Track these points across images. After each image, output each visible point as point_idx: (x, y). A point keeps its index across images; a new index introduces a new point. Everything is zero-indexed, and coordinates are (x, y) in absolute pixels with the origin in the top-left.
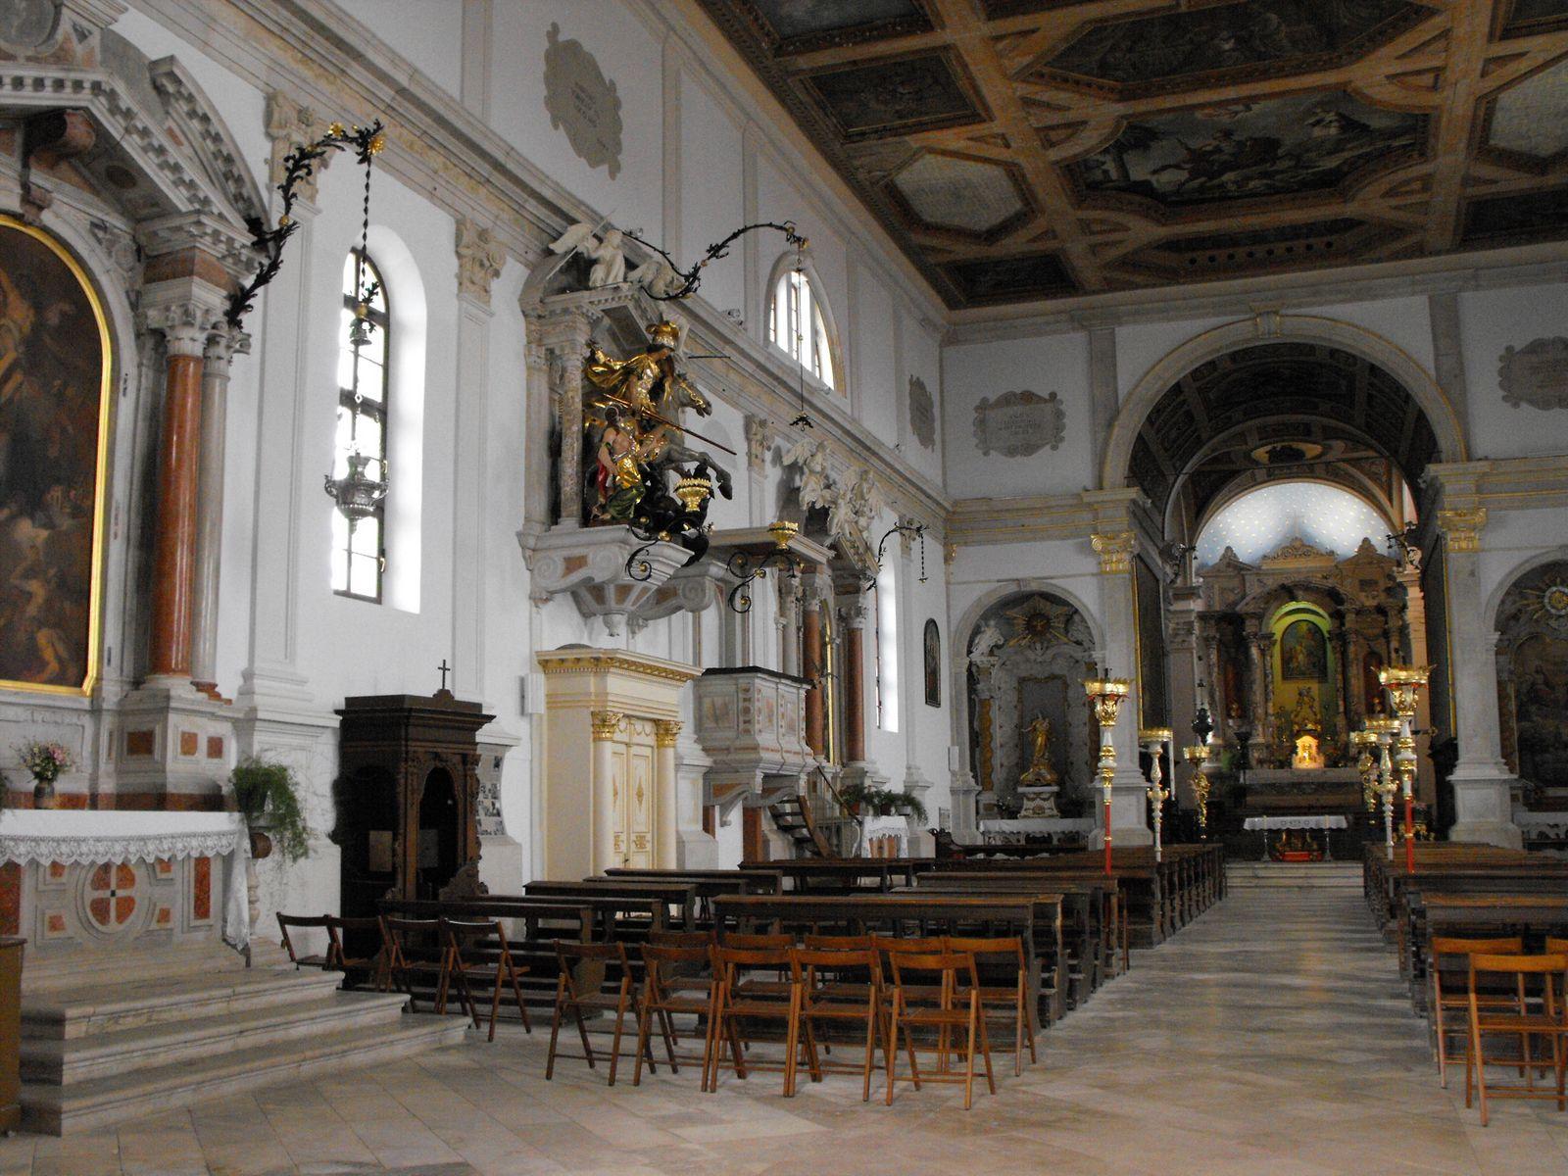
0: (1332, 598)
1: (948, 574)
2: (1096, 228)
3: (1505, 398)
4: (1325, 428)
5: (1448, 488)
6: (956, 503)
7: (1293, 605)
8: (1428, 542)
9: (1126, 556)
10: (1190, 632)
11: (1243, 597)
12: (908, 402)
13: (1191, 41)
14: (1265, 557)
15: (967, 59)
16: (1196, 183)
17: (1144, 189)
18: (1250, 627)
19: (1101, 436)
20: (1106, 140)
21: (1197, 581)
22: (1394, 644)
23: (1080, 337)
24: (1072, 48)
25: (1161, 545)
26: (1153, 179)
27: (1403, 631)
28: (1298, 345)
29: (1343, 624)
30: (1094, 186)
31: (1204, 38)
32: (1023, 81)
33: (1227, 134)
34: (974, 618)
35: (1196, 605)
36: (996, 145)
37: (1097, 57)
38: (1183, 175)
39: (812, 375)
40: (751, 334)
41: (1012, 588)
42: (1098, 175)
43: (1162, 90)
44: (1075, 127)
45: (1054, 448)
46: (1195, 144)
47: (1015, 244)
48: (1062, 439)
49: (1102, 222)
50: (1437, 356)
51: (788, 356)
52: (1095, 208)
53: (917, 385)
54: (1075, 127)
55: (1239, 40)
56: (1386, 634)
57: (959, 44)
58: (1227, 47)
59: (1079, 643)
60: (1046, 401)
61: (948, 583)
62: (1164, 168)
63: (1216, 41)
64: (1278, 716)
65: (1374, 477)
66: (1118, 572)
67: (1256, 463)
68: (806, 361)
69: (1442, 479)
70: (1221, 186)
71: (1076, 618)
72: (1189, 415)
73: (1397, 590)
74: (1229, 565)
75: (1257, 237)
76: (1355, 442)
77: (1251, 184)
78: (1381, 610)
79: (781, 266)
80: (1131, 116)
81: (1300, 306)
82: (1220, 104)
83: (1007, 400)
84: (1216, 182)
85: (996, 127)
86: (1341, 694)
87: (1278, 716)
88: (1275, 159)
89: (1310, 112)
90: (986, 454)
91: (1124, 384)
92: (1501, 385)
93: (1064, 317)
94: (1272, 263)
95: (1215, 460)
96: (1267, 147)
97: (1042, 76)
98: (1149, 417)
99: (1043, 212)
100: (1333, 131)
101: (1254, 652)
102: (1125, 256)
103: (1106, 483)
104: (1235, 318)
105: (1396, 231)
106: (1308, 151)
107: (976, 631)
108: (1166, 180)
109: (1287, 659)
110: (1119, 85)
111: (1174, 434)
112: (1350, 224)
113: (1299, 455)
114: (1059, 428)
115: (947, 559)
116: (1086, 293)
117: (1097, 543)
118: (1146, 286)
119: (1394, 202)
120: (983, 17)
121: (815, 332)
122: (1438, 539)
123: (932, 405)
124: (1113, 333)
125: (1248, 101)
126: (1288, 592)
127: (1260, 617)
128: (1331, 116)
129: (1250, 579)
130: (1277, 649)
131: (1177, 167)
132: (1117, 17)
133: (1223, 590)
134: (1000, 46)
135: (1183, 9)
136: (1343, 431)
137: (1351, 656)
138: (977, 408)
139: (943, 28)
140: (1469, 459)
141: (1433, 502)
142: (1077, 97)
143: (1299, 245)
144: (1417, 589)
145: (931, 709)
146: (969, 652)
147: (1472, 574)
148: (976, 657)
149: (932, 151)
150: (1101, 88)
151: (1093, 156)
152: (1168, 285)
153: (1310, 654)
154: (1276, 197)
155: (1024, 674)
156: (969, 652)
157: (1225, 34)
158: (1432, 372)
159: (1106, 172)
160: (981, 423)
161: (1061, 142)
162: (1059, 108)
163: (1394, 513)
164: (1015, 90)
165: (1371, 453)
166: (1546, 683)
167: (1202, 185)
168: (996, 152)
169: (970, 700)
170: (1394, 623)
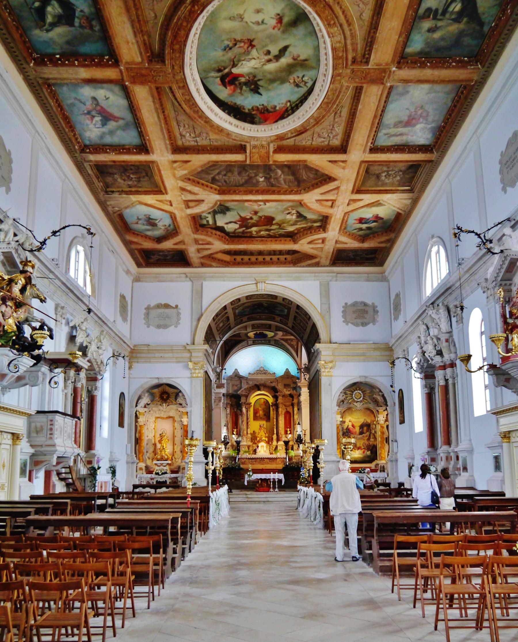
0: (274, 391)
1: (130, 374)
2: (201, 242)
3: (343, 321)
4: (276, 326)
5: (323, 353)
6: (135, 346)
7: (259, 392)
8: (313, 371)
9: (202, 371)
10: (220, 401)
11: (241, 388)
12: (119, 303)
13: (248, 175)
14: (249, 374)
15: (161, 168)
16: (241, 230)
17: (221, 229)
18: (243, 400)
19: (195, 324)
20: (211, 208)
21: (224, 381)
22: (296, 409)
23: (189, 284)
24: (202, 171)
25: (213, 367)
26: (226, 227)
27: (299, 403)
28: (271, 295)
29: (277, 400)
30: (203, 226)
31: (253, 175)
32: (183, 181)
33: (256, 213)
34: (139, 393)
35: (223, 391)
36: (167, 204)
37: (212, 176)
38: (237, 226)
39: (83, 288)
40: (60, 269)
41: (155, 382)
42: (205, 222)
43: (235, 193)
44: (200, 202)
45: (176, 327)
46: (243, 215)
47: (168, 245)
48: (179, 323)
49: (202, 240)
50: (321, 304)
51: (74, 280)
52: (202, 234)
53: (123, 297)
54: (200, 202)
55: (266, 178)
56: (293, 405)
57: (159, 162)
58: (262, 180)
59: (181, 404)
60: (173, 308)
61: (129, 378)
62: (231, 222)
63: (258, 177)
64: (251, 434)
65: (292, 346)
66: (198, 377)
67: (249, 338)
68: (81, 283)
69: (321, 349)
70: (251, 232)
71: (180, 394)
72: (228, 318)
73: (297, 388)
74: (236, 376)
75: (260, 253)
76: (287, 332)
77: (262, 233)
78: (291, 396)
79: (75, 241)
80: (220, 201)
81: (273, 280)
82: (256, 201)
83: (159, 306)
84: (249, 230)
85: (167, 197)
86: (275, 427)
87: (251, 434)
88: (272, 224)
89: (287, 209)
90: (148, 327)
91: (205, 305)
92: (343, 316)
93: (184, 276)
94: (265, 263)
95: (234, 336)
96: (269, 220)
97: (189, 179)
98: (213, 318)
99: (181, 233)
100: (294, 217)
101: (244, 410)
102: (212, 254)
103: (196, 343)
104: (249, 283)
105: (311, 257)
106: (284, 223)
107: (139, 398)
108: (231, 228)
109: (256, 412)
110: (218, 188)
111: (221, 325)
112: (295, 252)
113: (266, 335)
114: (179, 319)
115: (130, 368)
116: (193, 267)
117: (191, 365)
118: (217, 267)
119: (311, 246)
120: (170, 152)
121: (85, 272)
122: (318, 372)
123: (127, 305)
124: (202, 284)
125: (265, 201)
126: (258, 387)
127: (247, 397)
128: (294, 212)
129: (244, 382)
130: (252, 409)
131: (235, 223)
132: (222, 162)
133: (233, 385)
134: (175, 165)
135: (248, 162)
136: (283, 328)
137: (280, 412)
138: (145, 309)
139: (153, 154)
140: (331, 343)
141: (316, 357)
142: (201, 190)
143: (275, 258)
144: (307, 389)
145: (120, 428)
146: (136, 406)
147: (330, 385)
148: (138, 408)
149: (141, 203)
150: (212, 188)
151: (204, 215)
152: (225, 267)
153: (264, 411)
154: (270, 239)
155: (158, 416)
156: (136, 406)
157: (261, 175)
158: (319, 310)
159: (208, 221)
160: (147, 315)
161: (193, 207)
162: (194, 194)
163: (298, 360)
164: (178, 184)
165: (292, 337)
166: (353, 426)
167: (243, 231)
168: (167, 207)
169: (136, 426)
170: (295, 401)
